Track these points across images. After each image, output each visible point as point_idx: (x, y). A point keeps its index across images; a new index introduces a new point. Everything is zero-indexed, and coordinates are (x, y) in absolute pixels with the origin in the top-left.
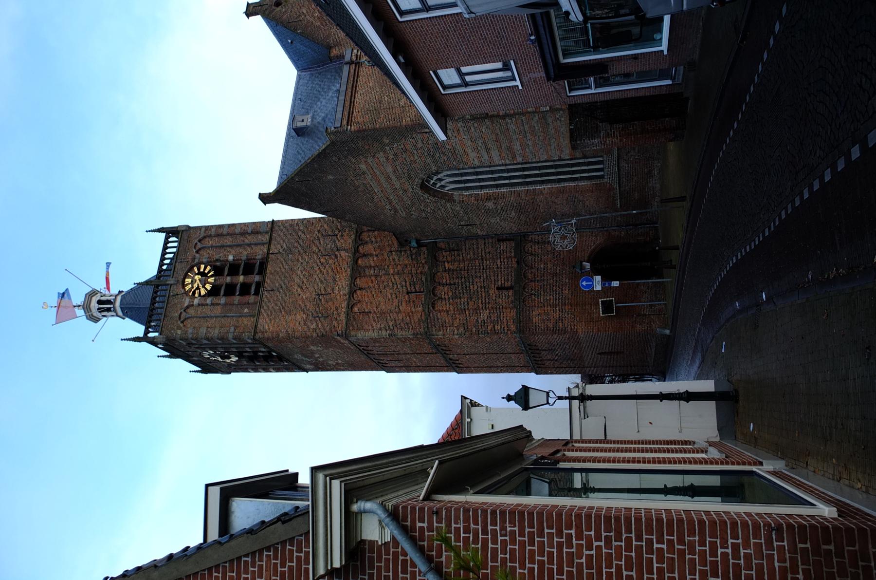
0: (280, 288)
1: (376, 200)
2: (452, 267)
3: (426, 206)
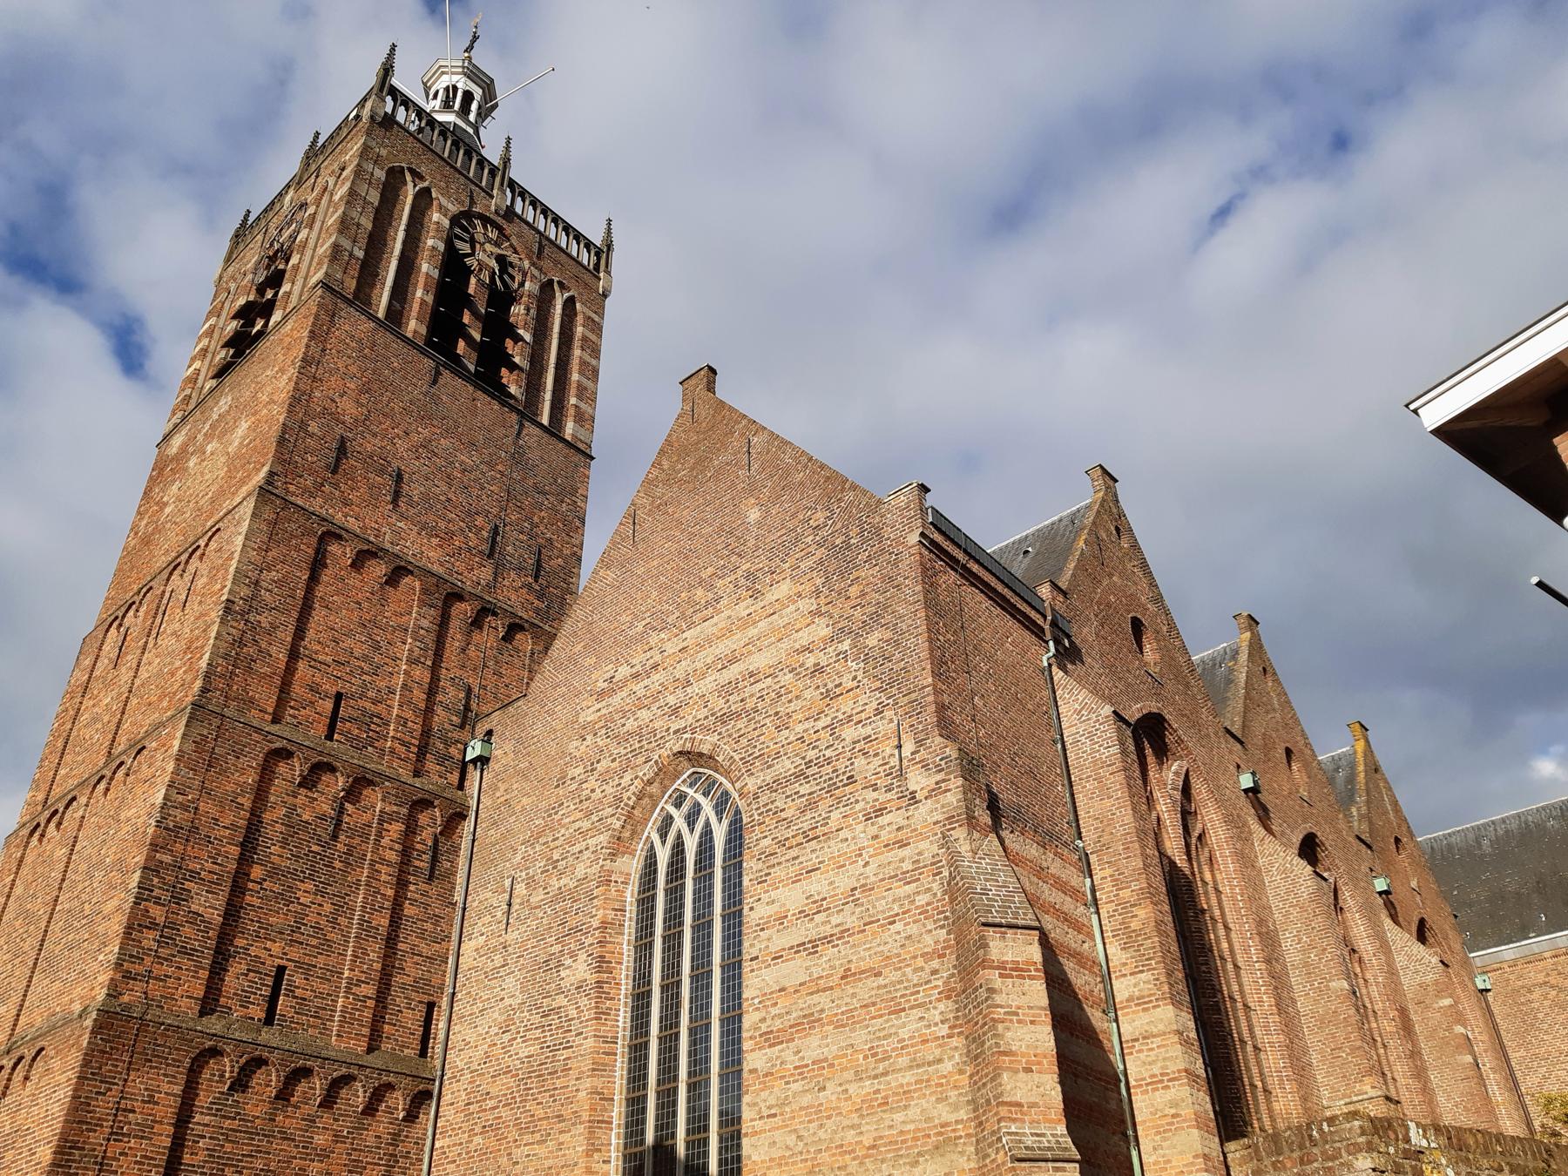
0: (436, 400)
1: (654, 639)
2: (385, 841)
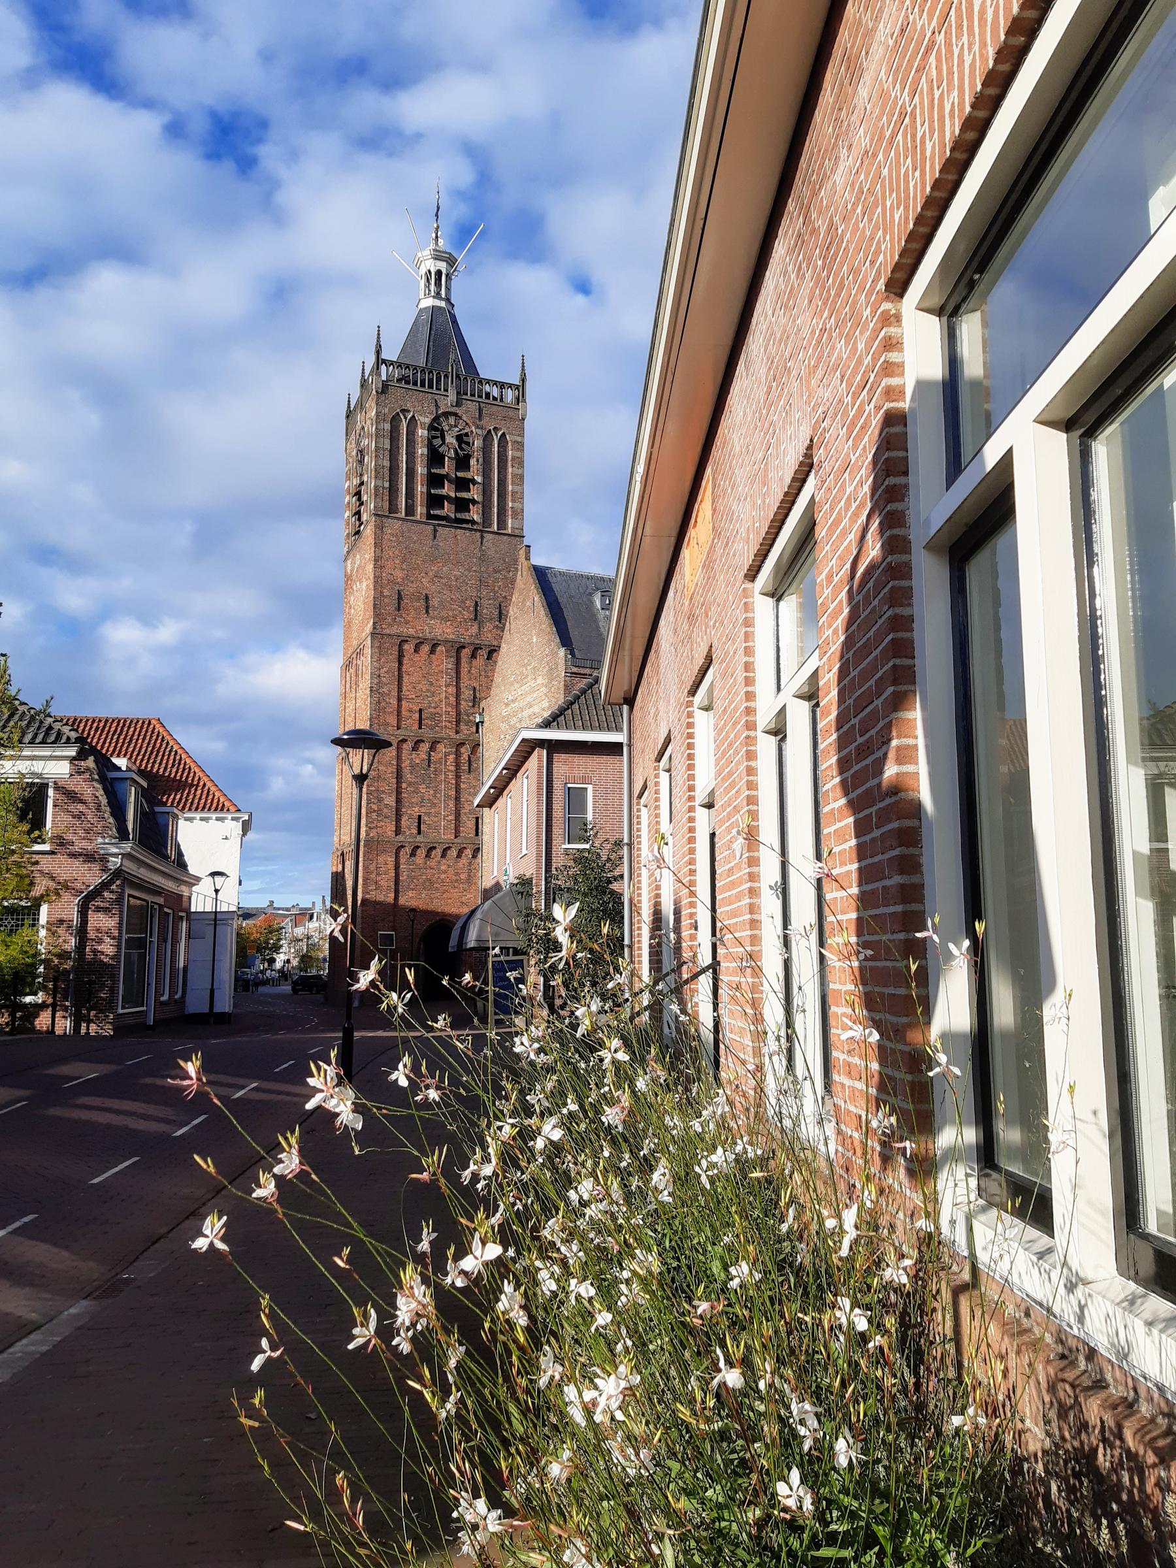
0: (437, 547)
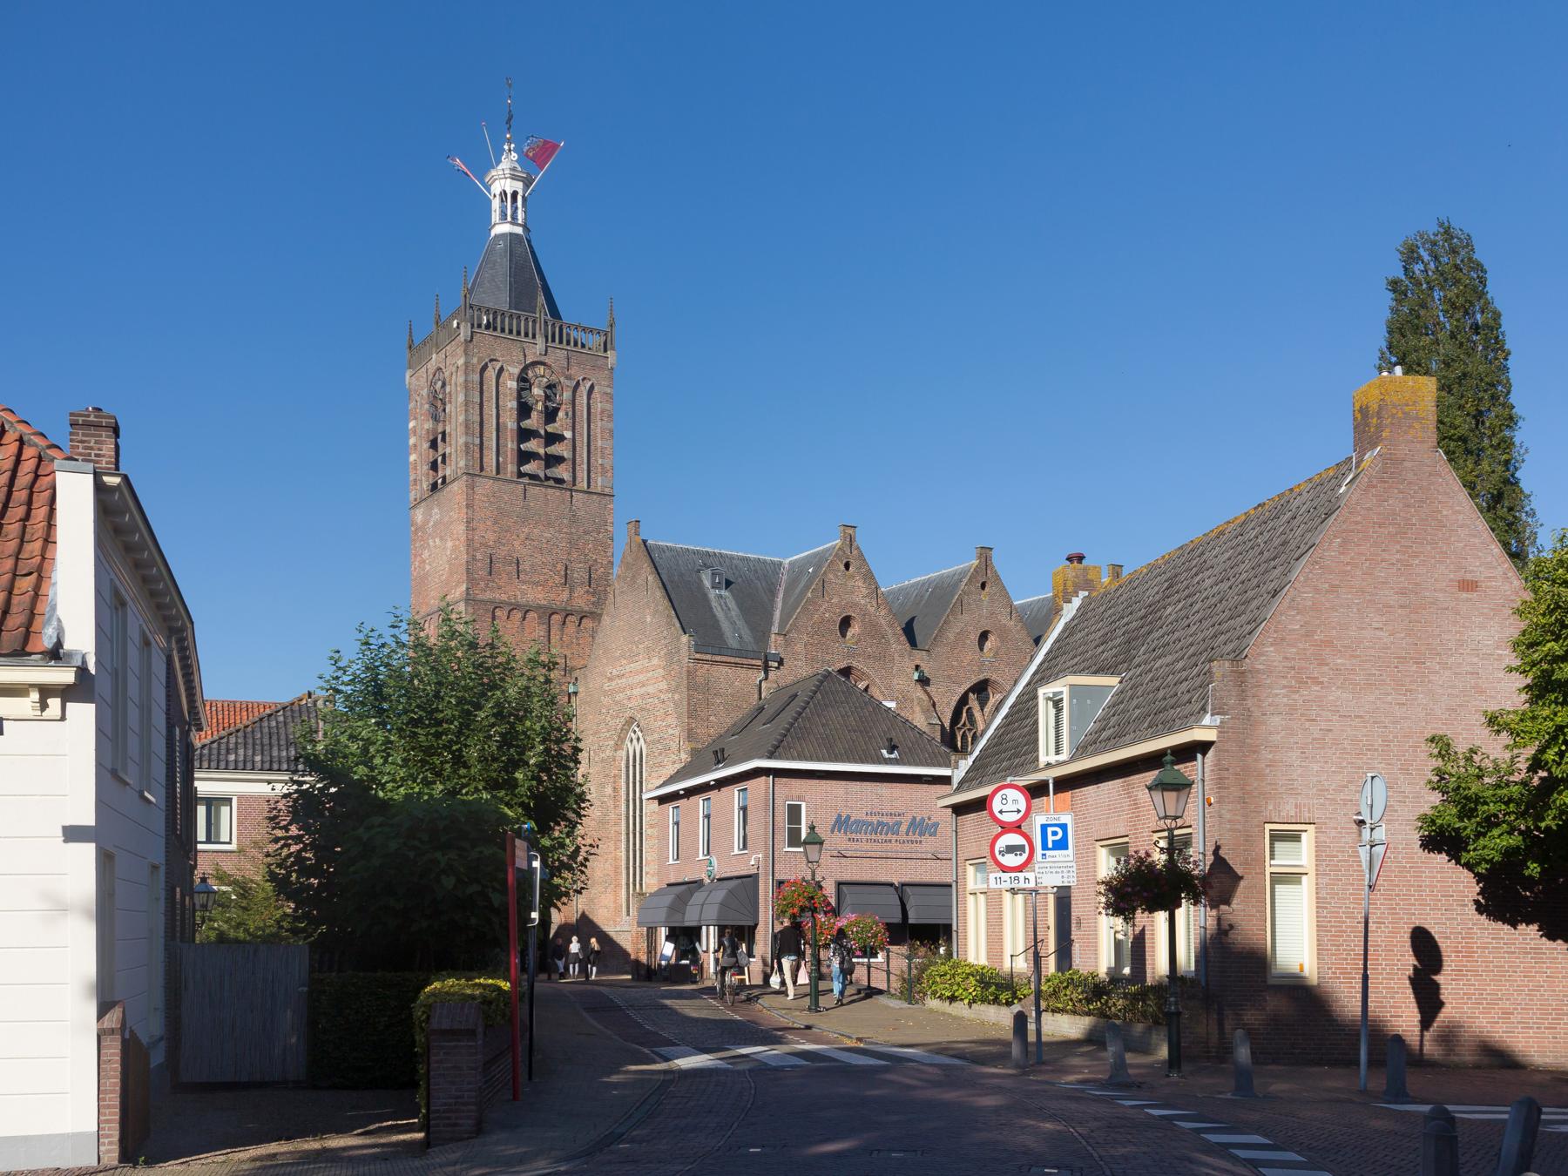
3: (613, 717)
